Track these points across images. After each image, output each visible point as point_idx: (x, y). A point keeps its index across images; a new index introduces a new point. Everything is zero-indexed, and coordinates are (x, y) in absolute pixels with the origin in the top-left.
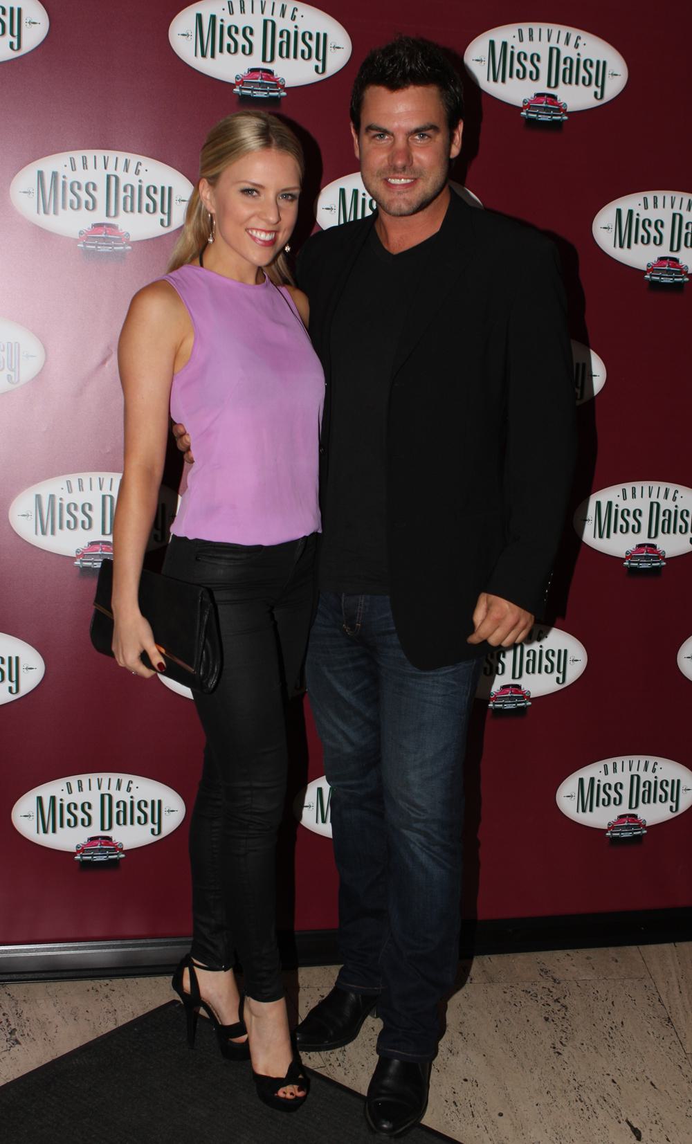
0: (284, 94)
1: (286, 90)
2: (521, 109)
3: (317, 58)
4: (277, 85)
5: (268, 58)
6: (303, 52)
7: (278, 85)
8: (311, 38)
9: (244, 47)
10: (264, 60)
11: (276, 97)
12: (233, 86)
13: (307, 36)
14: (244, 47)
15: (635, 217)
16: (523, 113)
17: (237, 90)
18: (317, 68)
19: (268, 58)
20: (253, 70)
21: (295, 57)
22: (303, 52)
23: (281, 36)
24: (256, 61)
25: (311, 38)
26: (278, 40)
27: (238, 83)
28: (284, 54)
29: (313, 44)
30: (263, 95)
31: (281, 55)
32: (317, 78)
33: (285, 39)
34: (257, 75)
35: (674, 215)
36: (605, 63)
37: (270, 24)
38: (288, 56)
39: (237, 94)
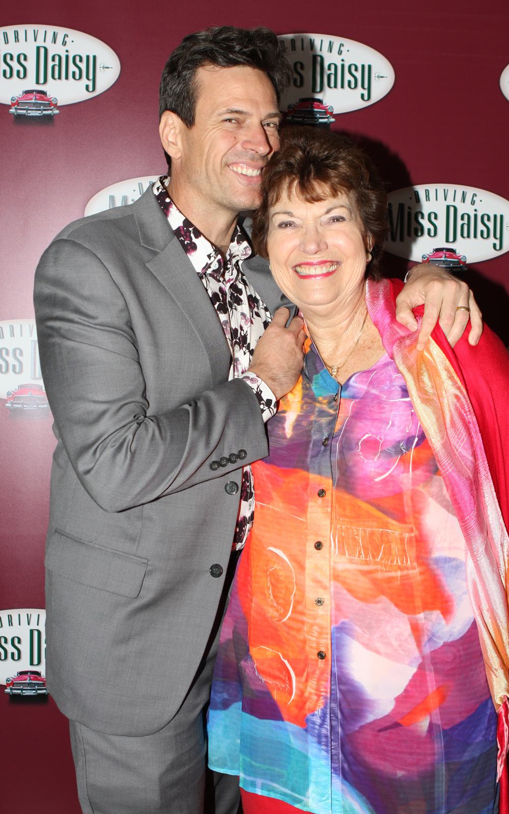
0: (57, 112)
1: (59, 108)
3: (88, 78)
4: (50, 104)
5: (42, 80)
6: (74, 73)
7: (51, 104)
9: (18, 72)
10: (38, 82)
11: (49, 116)
12: (9, 107)
13: (78, 59)
14: (18, 72)
15: (406, 210)
17: (12, 110)
18: (87, 87)
20: (28, 92)
21: (67, 78)
23: (53, 60)
24: (30, 83)
27: (13, 105)
28: (56, 76)
29: (83, 66)
31: (53, 77)
34: (31, 96)
35: (448, 207)
36: (370, 67)
38: (60, 78)
39: (13, 114)
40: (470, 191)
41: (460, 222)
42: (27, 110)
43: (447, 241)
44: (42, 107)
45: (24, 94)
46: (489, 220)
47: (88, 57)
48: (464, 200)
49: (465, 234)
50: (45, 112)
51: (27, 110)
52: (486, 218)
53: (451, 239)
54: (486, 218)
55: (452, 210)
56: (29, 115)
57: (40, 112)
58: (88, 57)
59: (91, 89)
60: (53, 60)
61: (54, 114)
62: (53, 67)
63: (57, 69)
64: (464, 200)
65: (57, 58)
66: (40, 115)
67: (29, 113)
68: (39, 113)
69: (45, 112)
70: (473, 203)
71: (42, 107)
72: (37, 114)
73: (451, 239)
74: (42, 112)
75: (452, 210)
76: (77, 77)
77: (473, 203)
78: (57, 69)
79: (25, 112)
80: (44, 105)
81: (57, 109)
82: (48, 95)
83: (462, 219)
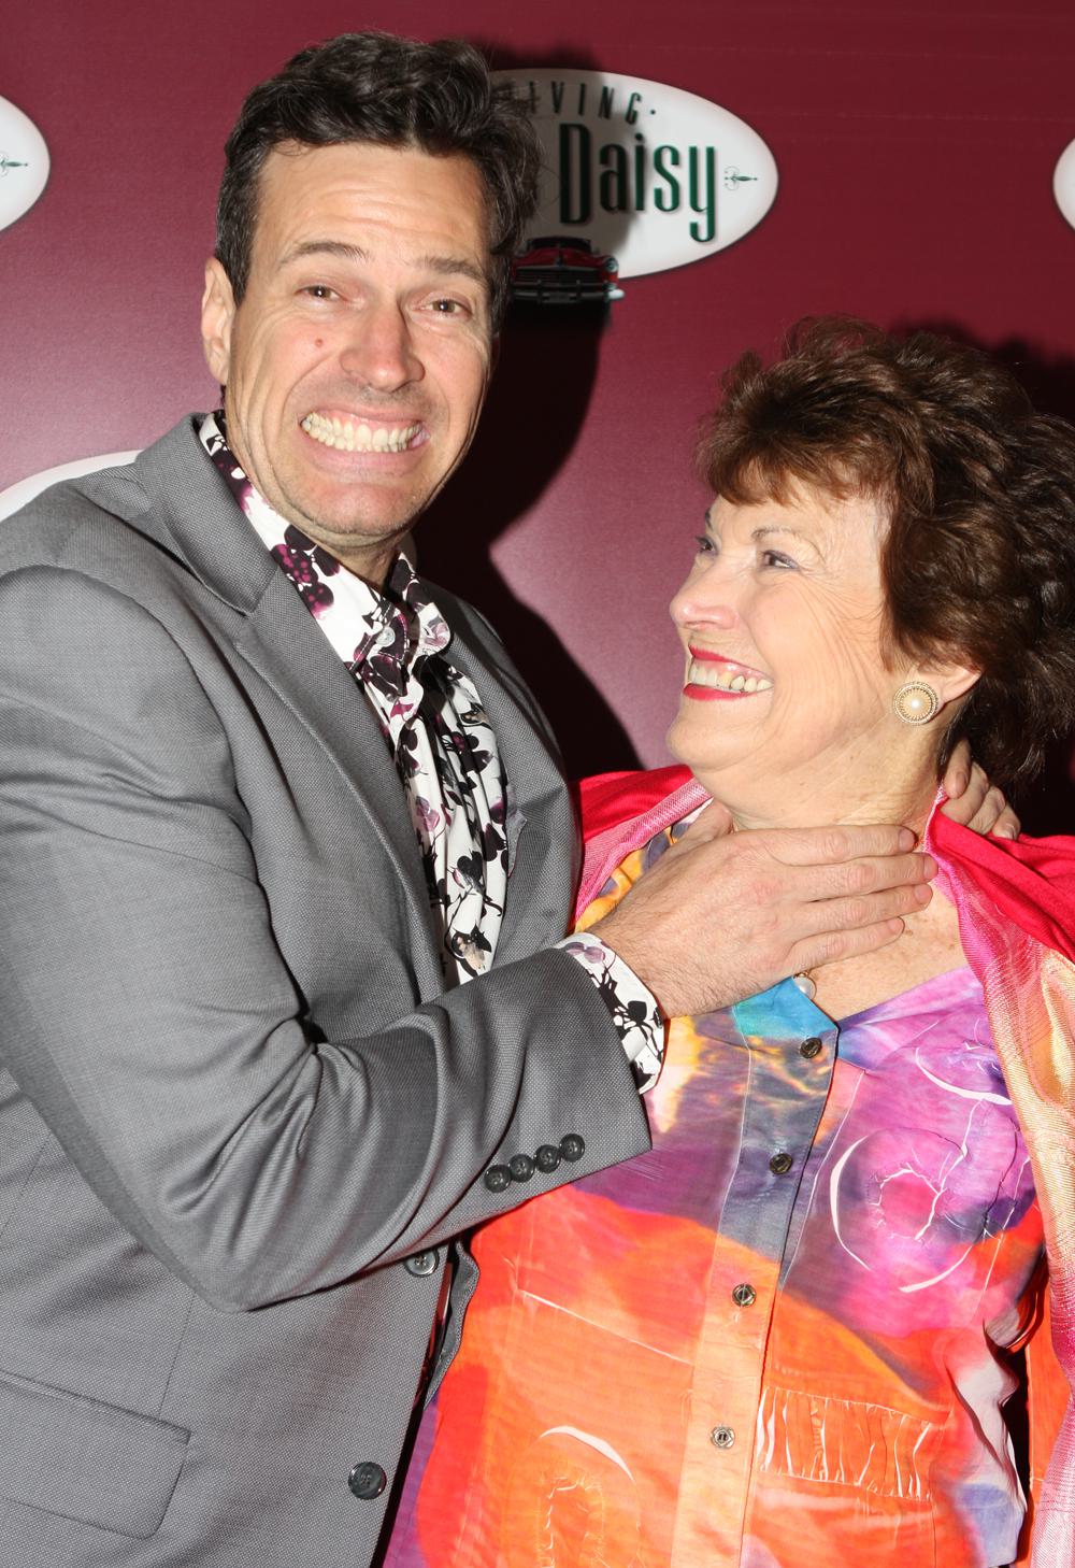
3: (695, 206)
5: (576, 214)
6: (659, 194)
8: (676, 161)
10: (565, 217)
18: (694, 229)
19: (576, 214)
22: (659, 194)
23: (605, 159)
25: (676, 161)
26: (598, 170)
28: (614, 202)
29: (682, 174)
30: (568, 298)
31: (606, 204)
32: (696, 252)
33: (614, 167)
37: (576, 136)
42: (540, 289)
44: (578, 282)
45: (531, 248)
47: (694, 152)
50: (585, 295)
51: (540, 289)
56: (546, 301)
57: (573, 295)
58: (694, 152)
59: (703, 234)
60: (605, 159)
62: (605, 178)
63: (614, 182)
65: (614, 155)
66: (573, 301)
67: (547, 298)
68: (572, 298)
69: (585, 295)
71: (578, 282)
72: (567, 301)
74: (579, 294)
76: (668, 203)
78: (614, 182)
79: (534, 294)
80: (584, 276)
81: (618, 288)
82: (593, 249)
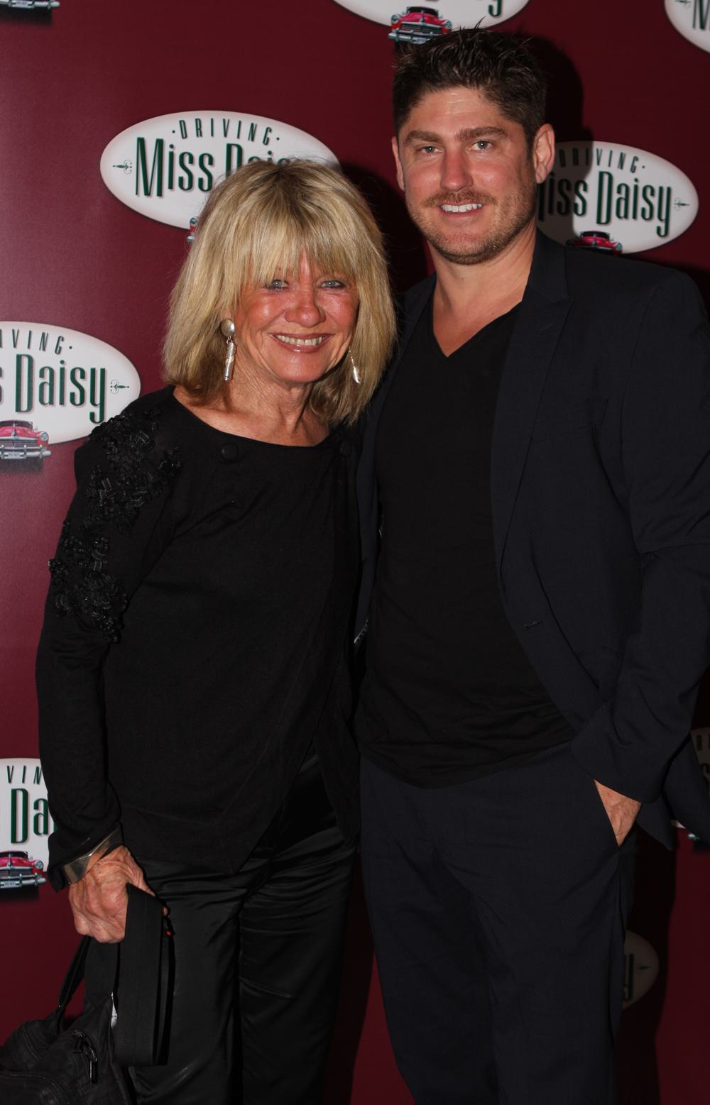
2: (388, 29)
16: (393, 35)
40: (630, 152)
41: (615, 196)
43: (599, 222)
46: (652, 194)
48: (621, 165)
49: (622, 214)
52: (649, 191)
53: (604, 219)
54: (649, 191)
55: (606, 178)
61: (53, 8)
64: (621, 165)
66: (30, 7)
68: (29, 5)
70: (633, 169)
73: (604, 219)
75: (606, 178)
77: (633, 169)
83: (619, 192)
